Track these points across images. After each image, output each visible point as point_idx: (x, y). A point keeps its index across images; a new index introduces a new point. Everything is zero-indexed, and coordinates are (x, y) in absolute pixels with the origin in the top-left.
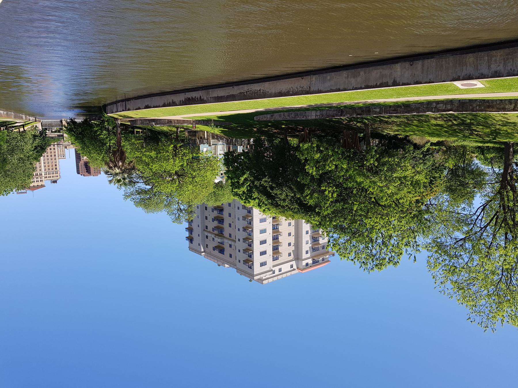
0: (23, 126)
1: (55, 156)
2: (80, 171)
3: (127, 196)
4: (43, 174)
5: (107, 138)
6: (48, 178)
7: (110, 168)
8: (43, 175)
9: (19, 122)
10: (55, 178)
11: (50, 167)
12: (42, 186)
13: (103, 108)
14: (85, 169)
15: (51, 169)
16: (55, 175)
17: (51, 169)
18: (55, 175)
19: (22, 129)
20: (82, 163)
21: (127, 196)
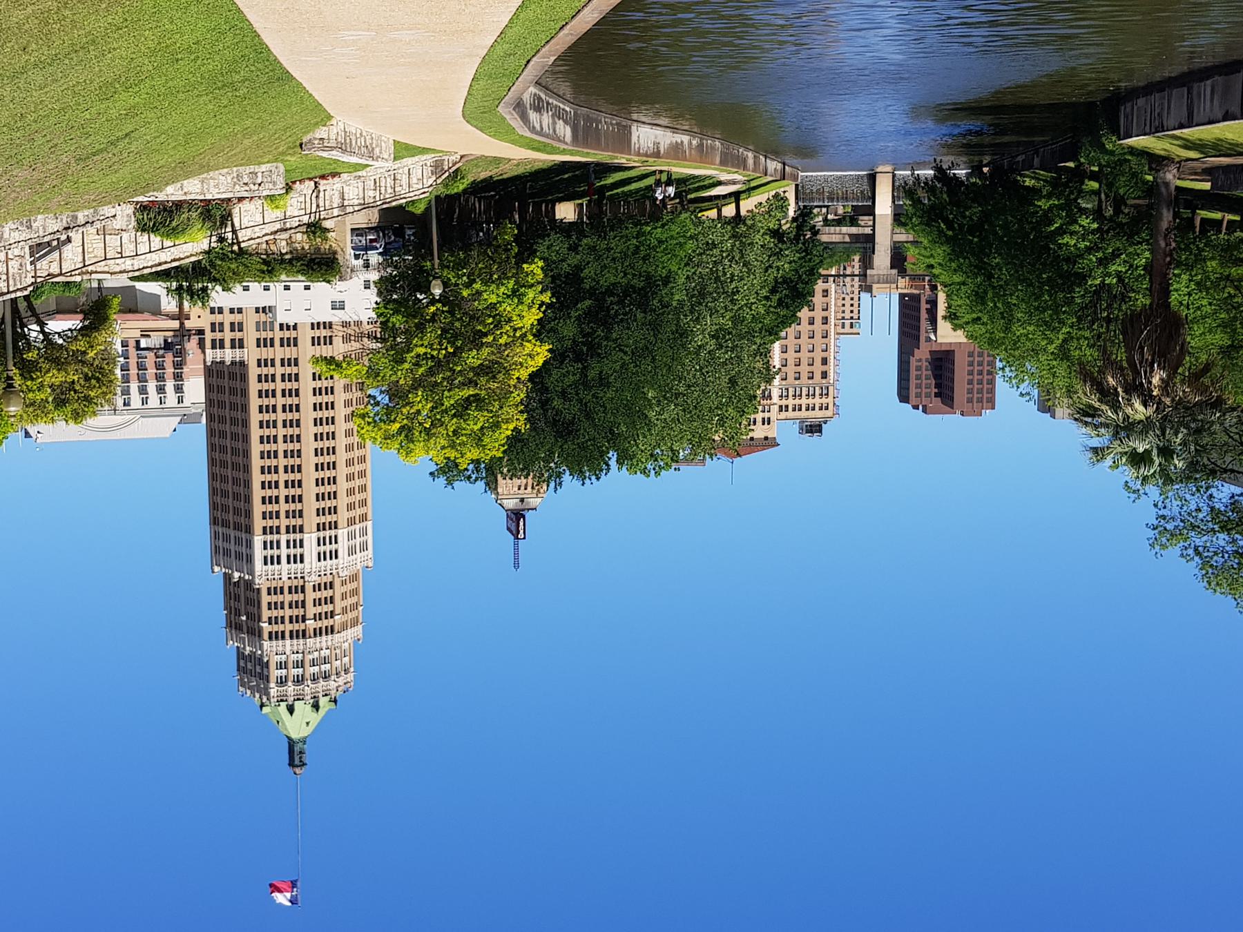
0: (736, 196)
1: (825, 321)
2: (913, 391)
3: (1167, 532)
4: (775, 393)
5: (1089, 250)
6: (790, 414)
7: (1107, 395)
8: (775, 399)
9: (729, 179)
10: (818, 414)
11: (804, 369)
12: (769, 443)
13: (1105, 111)
14: (934, 381)
15: (804, 376)
16: (817, 401)
17: (804, 376)
18: (817, 401)
19: (729, 211)
20: (922, 354)
21: (1167, 532)
